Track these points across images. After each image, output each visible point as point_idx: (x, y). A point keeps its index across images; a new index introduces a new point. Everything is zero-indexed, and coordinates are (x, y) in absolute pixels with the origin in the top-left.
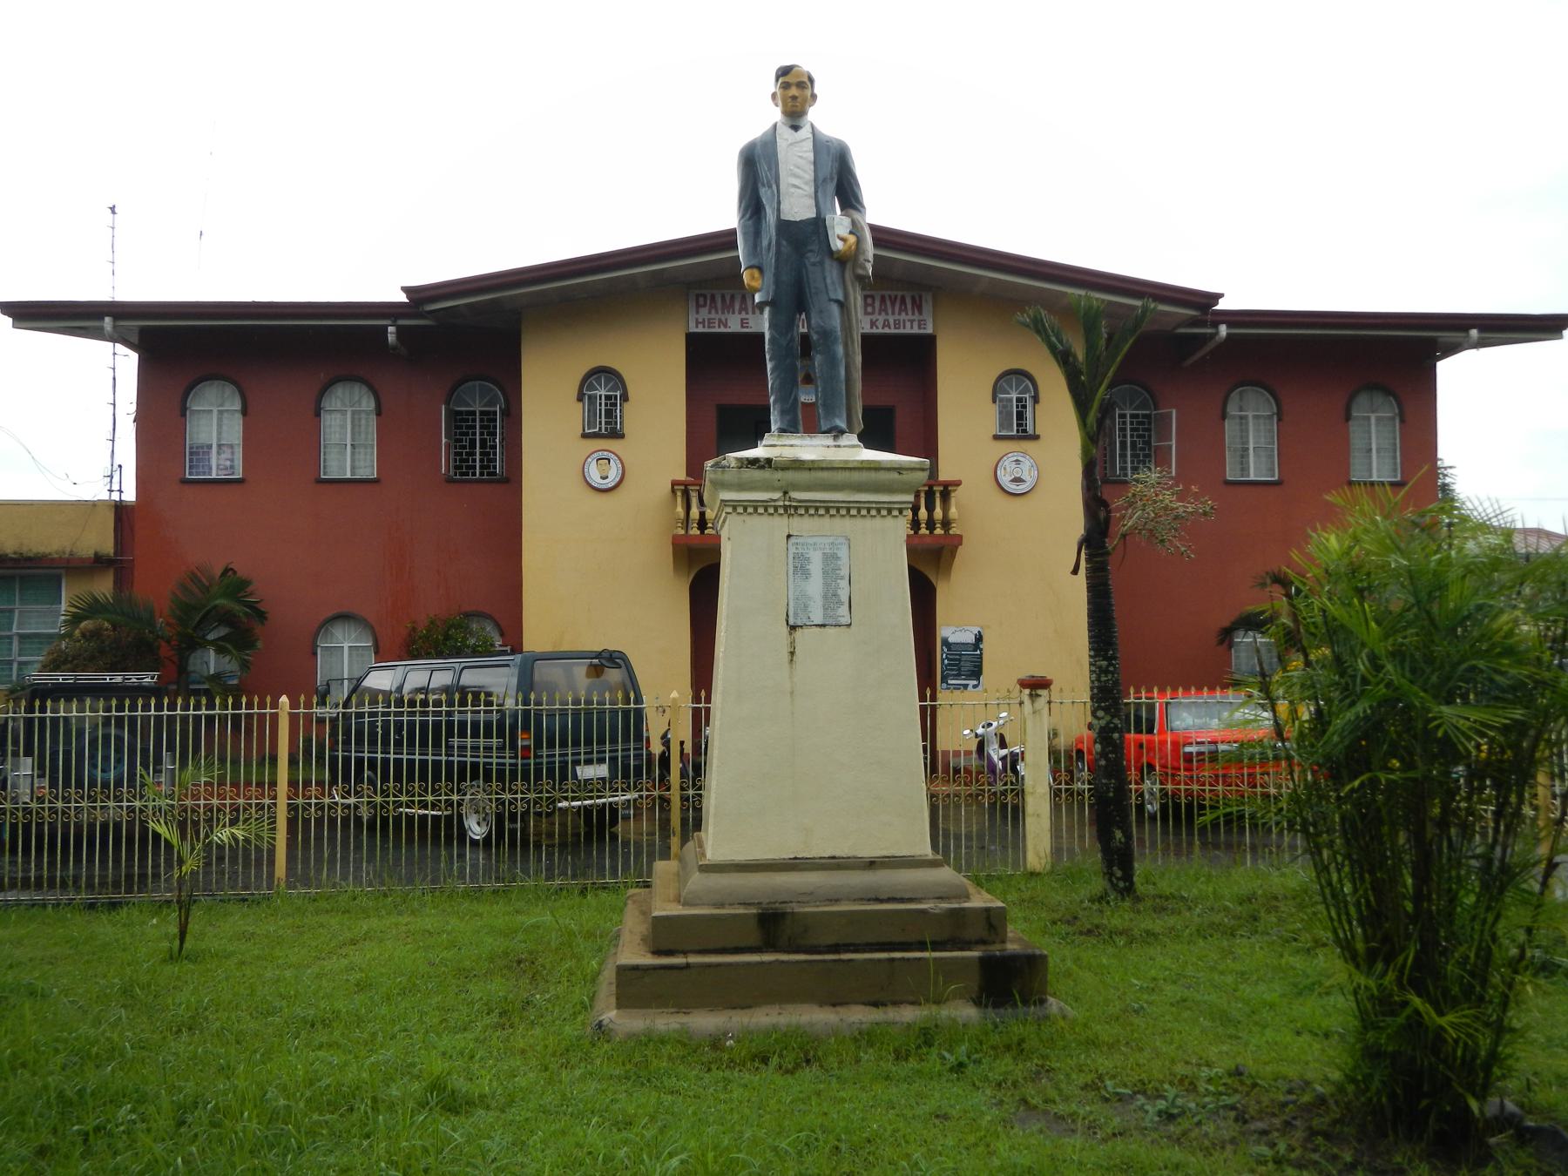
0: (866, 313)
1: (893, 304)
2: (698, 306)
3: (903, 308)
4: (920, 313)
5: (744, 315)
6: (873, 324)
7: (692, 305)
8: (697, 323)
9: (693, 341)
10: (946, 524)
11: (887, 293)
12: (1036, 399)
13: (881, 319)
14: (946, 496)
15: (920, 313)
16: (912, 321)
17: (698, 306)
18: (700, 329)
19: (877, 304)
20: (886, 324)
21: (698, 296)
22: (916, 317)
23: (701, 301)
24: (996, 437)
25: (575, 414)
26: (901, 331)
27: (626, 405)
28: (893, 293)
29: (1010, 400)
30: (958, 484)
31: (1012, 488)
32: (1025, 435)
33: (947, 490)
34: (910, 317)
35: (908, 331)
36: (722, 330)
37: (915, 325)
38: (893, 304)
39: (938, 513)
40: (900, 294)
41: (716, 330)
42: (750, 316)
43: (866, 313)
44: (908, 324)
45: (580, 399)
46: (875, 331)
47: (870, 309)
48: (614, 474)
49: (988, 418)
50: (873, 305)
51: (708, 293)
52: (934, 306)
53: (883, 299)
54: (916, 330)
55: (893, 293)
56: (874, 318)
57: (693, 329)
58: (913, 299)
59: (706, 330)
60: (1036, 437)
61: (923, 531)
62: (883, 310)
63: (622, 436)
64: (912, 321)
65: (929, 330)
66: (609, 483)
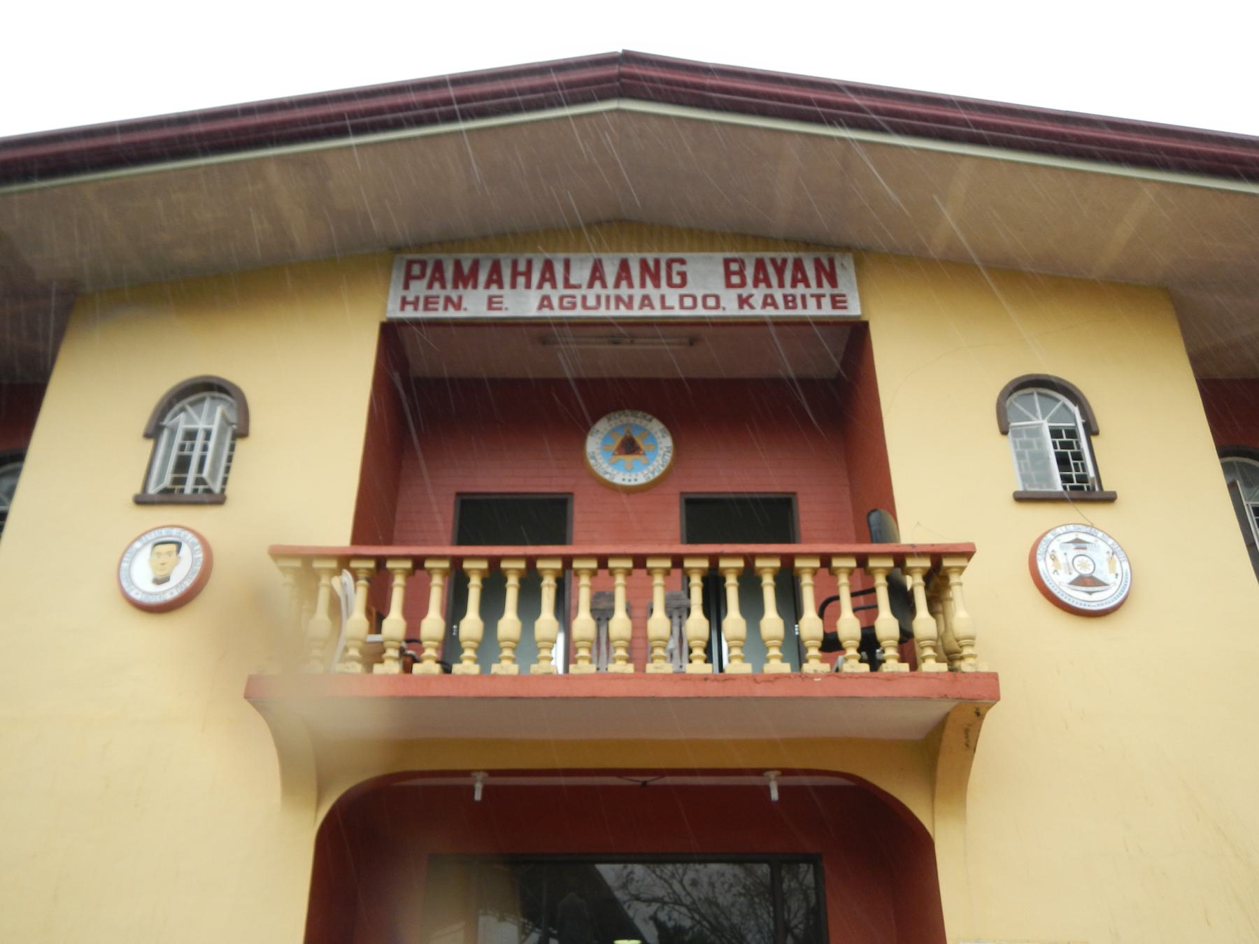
0: (729, 285)
1: (780, 272)
2: (409, 278)
3: (800, 277)
4: (834, 284)
5: (494, 290)
6: (743, 301)
7: (398, 276)
8: (404, 302)
9: (392, 336)
10: (951, 656)
11: (767, 256)
12: (1091, 430)
13: (758, 294)
14: (937, 581)
15: (834, 284)
16: (818, 297)
17: (409, 278)
18: (409, 313)
19: (749, 272)
20: (769, 301)
21: (410, 264)
22: (827, 289)
23: (416, 270)
24: (1021, 498)
25: (131, 461)
26: (799, 312)
27: (240, 444)
28: (778, 256)
29: (1036, 432)
30: (968, 554)
31: (1078, 597)
32: (1083, 490)
33: (939, 570)
34: (814, 289)
35: (812, 311)
36: (451, 313)
37: (826, 302)
38: (780, 272)
39: (924, 623)
40: (791, 256)
41: (440, 314)
42: (507, 291)
43: (729, 285)
44: (812, 302)
45: (154, 432)
46: (746, 312)
47: (735, 280)
48: (182, 574)
49: (997, 465)
50: (741, 273)
51: (430, 258)
52: (858, 276)
53: (760, 265)
54: (827, 310)
55: (778, 256)
56: (745, 292)
57: (394, 311)
58: (818, 263)
59: (421, 314)
60: (1110, 499)
61: (892, 664)
62: (761, 277)
63: (218, 500)
64: (818, 297)
65: (854, 309)
66: (168, 592)
